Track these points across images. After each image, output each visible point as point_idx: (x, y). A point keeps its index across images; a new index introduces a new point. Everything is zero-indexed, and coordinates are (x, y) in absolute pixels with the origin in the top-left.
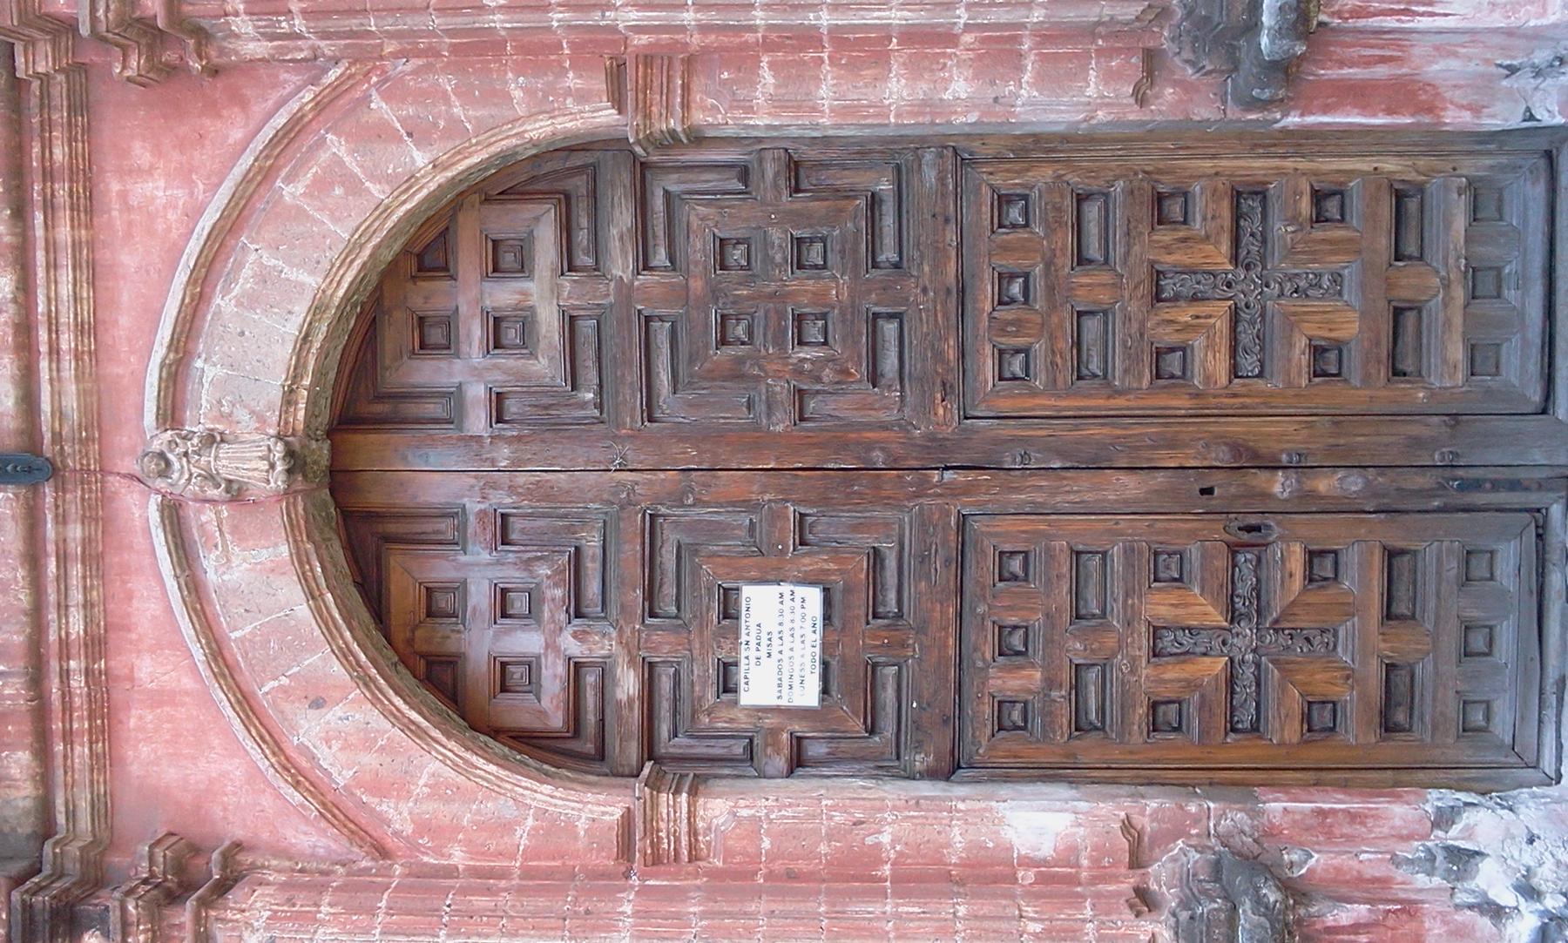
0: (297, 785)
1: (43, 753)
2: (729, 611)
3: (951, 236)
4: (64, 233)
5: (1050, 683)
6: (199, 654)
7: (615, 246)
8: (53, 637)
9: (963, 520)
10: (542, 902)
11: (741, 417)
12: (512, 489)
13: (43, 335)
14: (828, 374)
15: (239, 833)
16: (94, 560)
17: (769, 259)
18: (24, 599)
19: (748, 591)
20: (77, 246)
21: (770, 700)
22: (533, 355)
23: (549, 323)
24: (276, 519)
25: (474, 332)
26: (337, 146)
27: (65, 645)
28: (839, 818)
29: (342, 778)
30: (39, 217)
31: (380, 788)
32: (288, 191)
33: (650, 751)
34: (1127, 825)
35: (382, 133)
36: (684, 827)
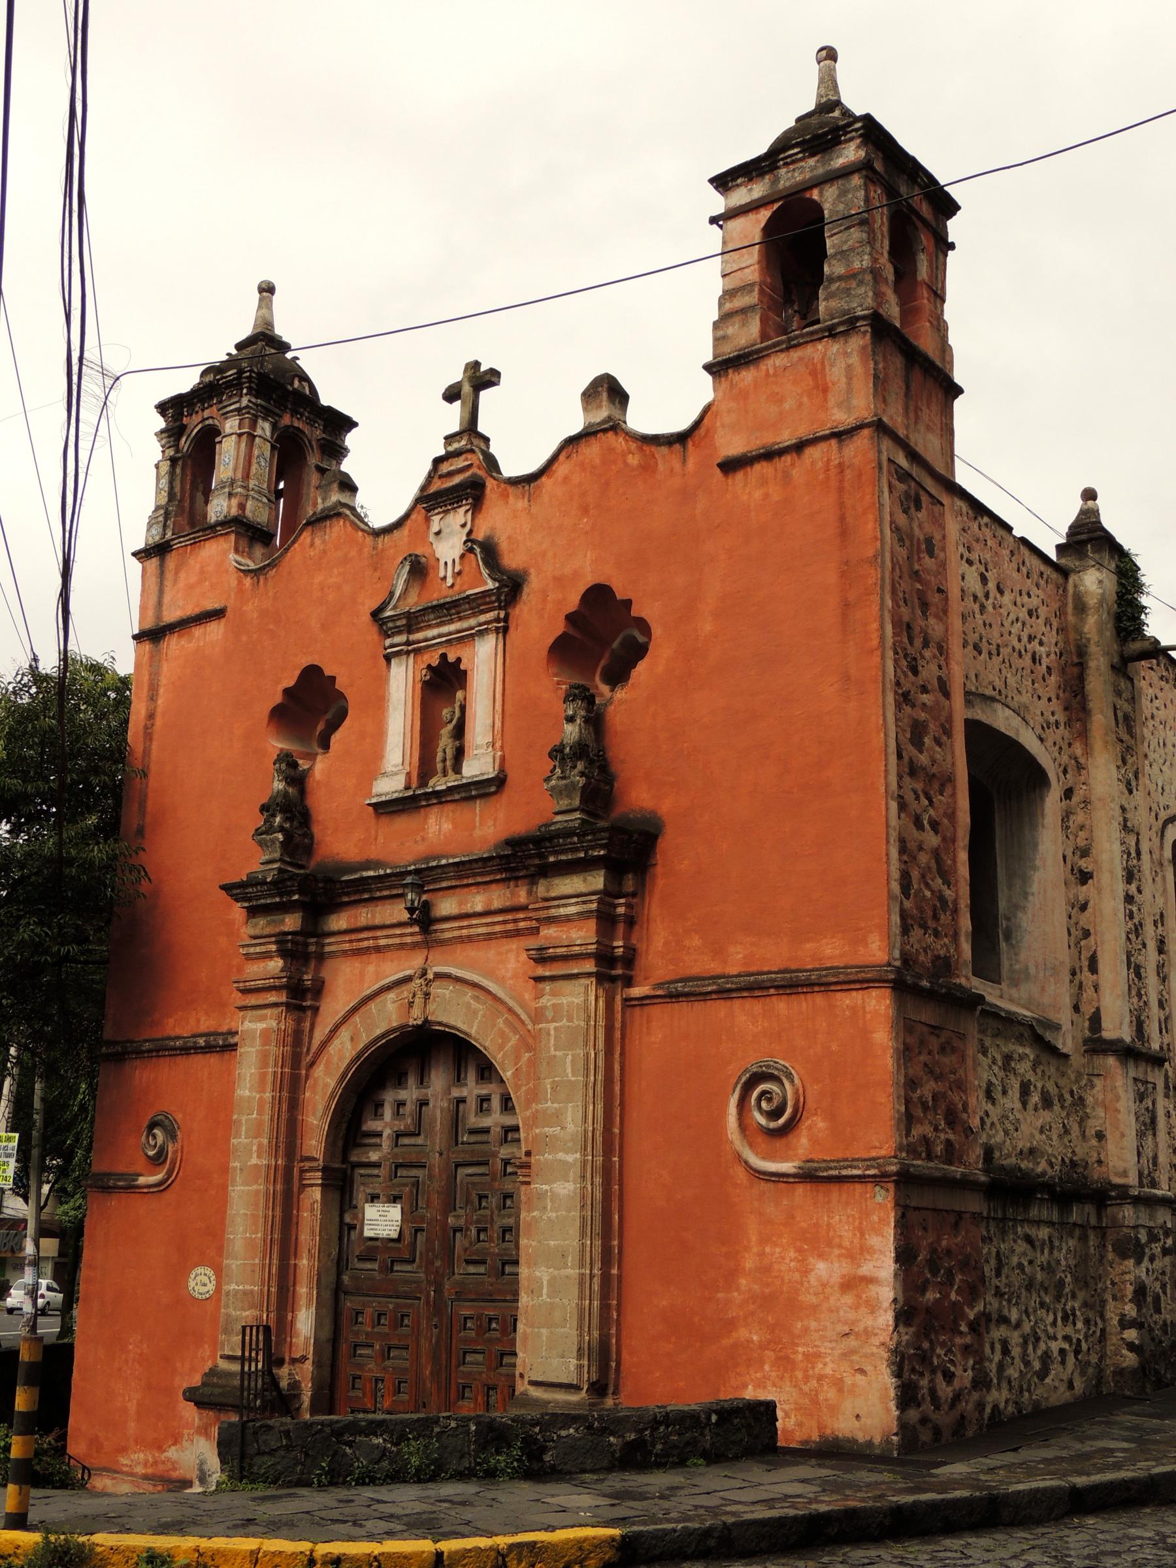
0: (331, 1031)
2: (395, 1199)
5: (367, 1334)
6: (368, 992)
7: (510, 1150)
8: (379, 933)
10: (283, 1129)
11: (458, 1206)
13: (465, 923)
15: (321, 1009)
16: (402, 946)
17: (504, 1217)
18: (388, 923)
19: (399, 1206)
20: (494, 933)
21: (367, 1216)
22: (476, 1114)
23: (486, 1122)
24: (403, 1021)
25: (484, 1092)
26: (514, 1040)
27: (376, 938)
30: (500, 918)
31: (328, 1063)
32: (500, 1021)
34: (303, 1359)
36: (312, 1182)
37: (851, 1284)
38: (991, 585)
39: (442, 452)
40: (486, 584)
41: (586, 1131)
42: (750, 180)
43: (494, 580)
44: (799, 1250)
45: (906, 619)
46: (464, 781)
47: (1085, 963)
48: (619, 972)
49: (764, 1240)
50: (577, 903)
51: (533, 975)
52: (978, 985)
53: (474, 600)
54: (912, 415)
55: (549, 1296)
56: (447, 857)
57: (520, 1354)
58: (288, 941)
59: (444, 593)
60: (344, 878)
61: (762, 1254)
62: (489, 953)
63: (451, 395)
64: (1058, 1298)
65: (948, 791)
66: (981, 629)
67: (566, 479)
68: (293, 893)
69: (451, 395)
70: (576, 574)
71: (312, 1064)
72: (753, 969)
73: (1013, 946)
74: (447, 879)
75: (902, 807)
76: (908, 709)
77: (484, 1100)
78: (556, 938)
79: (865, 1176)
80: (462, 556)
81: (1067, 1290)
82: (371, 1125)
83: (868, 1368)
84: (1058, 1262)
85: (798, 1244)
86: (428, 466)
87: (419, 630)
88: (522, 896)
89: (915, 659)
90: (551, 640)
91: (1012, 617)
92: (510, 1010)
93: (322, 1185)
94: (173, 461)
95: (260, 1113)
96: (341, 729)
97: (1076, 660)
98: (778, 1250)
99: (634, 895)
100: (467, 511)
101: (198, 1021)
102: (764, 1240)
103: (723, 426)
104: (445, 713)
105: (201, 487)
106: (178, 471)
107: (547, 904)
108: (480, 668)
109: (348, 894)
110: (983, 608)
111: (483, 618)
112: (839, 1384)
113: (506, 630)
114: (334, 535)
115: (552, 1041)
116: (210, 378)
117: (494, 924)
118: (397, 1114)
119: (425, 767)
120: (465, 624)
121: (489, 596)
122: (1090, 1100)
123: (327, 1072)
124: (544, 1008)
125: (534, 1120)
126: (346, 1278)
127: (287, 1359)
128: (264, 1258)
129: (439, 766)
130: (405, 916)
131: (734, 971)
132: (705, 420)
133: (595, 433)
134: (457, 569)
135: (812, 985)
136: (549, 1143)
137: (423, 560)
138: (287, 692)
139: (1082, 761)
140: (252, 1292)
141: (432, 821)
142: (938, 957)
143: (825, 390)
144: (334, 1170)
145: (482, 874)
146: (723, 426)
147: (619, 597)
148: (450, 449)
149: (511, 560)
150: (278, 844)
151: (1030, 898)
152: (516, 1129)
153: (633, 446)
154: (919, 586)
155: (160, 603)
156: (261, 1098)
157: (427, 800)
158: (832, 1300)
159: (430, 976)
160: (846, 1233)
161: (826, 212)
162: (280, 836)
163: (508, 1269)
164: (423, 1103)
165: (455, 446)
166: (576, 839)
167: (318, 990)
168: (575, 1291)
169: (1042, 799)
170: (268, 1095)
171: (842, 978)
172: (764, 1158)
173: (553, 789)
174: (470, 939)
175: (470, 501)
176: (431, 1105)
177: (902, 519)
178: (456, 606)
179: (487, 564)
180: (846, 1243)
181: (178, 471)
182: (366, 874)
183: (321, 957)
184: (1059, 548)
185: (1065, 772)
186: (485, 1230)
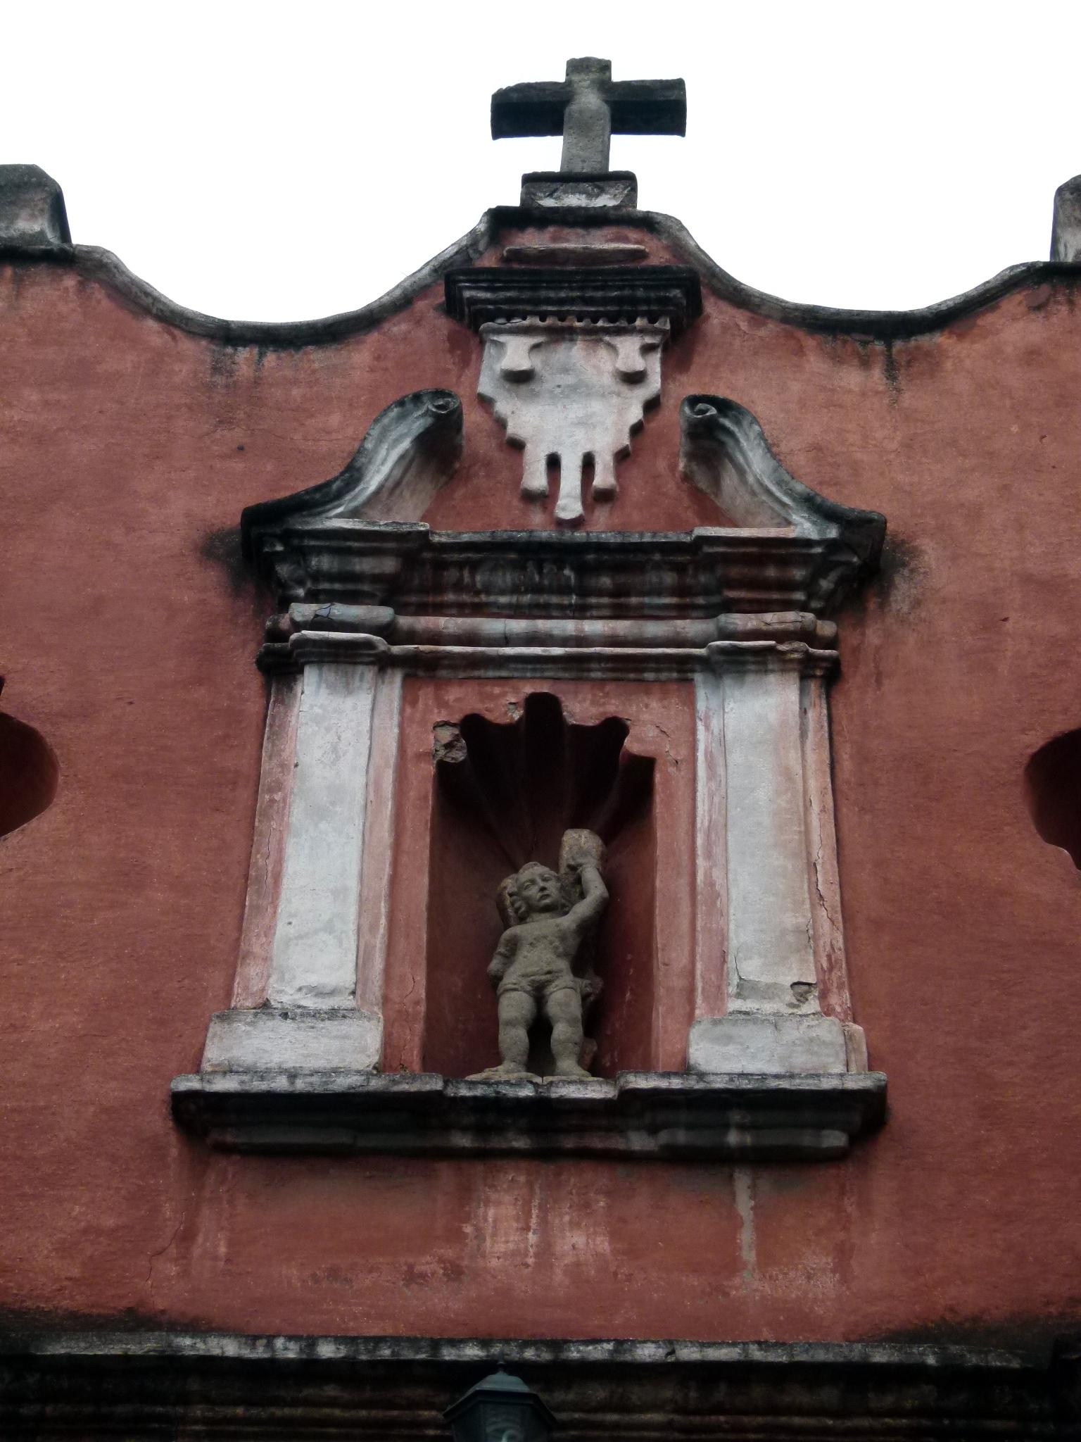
53: (726, 559)
60: (59, 1349)
80: (622, 457)
90: (1036, 740)
121: (784, 562)
134: (603, 478)
157: (481, 1130)
175: (665, 324)
178: (616, 569)
182: (187, 1344)
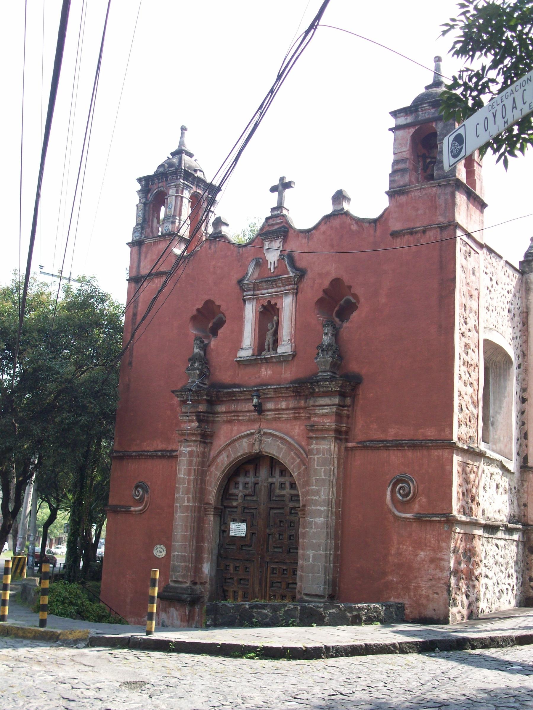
1: (225, 413)
2: (243, 521)
3: (292, 561)
4: (291, 415)
5: (231, 574)
6: (235, 438)
7: (294, 504)
8: (239, 414)
9: (253, 561)
11: (271, 525)
12: (261, 485)
13: (277, 413)
14: (274, 539)
15: (214, 443)
16: (249, 420)
18: (244, 410)
22: (279, 489)
23: (284, 492)
25: (282, 480)
26: (298, 460)
27: (238, 416)
28: (209, 537)
29: (218, 460)
31: (217, 466)
32: (292, 453)
33: (225, 507)
34: (206, 583)
35: (299, 468)
37: (432, 560)
38: (494, 282)
39: (269, 215)
40: (289, 274)
41: (329, 499)
42: (407, 115)
43: (293, 272)
44: (413, 547)
45: (464, 303)
46: (278, 355)
47: (523, 435)
48: (344, 437)
49: (399, 543)
50: (328, 409)
51: (308, 436)
52: (483, 447)
54: (469, 218)
55: (312, 561)
56: (271, 385)
57: (299, 584)
58: (200, 416)
59: (270, 275)
61: (398, 548)
62: (287, 426)
63: (273, 189)
64: (506, 569)
65: (477, 369)
66: (489, 301)
67: (324, 233)
68: (202, 396)
69: (273, 189)
70: (328, 274)
71: (209, 466)
72: (398, 438)
73: (494, 428)
74: (270, 394)
75: (460, 378)
76: (463, 338)
77: (282, 484)
78: (318, 422)
79: (441, 520)
80: (278, 260)
81: (510, 566)
82: (233, 491)
83: (439, 592)
84: (507, 555)
85: (413, 545)
86: (263, 221)
87: (259, 290)
88: (302, 403)
89: (466, 318)
90: (316, 299)
91: (502, 294)
92: (296, 449)
93: (214, 514)
94: (145, 204)
95: (189, 484)
96: (223, 328)
97: (525, 310)
98: (405, 547)
99: (349, 406)
100: (280, 242)
101: (158, 445)
102: (399, 543)
103: (392, 218)
104: (269, 325)
105: (156, 215)
106: (147, 209)
107: (314, 408)
108: (286, 308)
109: (226, 397)
110: (490, 291)
111: (287, 288)
112: (427, 598)
113: (297, 293)
114: (220, 245)
115: (316, 463)
116: (161, 170)
117: (289, 414)
118: (245, 488)
119: (260, 347)
120: (279, 290)
122: (522, 491)
123: (216, 469)
124: (312, 449)
125: (307, 493)
126: (222, 551)
127: (198, 582)
128: (190, 542)
129: (266, 347)
130: (253, 408)
131: (391, 439)
132: (385, 215)
133: (337, 215)
135: (422, 446)
136: (315, 503)
137: (261, 260)
138: (198, 310)
139: (526, 352)
140: (185, 556)
141: (263, 369)
142: (470, 437)
143: (436, 208)
144: (219, 509)
145: (285, 393)
146: (392, 218)
147: (346, 284)
148: (273, 214)
149: (301, 264)
150: (196, 375)
151: (503, 409)
152: (298, 496)
153: (354, 222)
154: (469, 288)
155: (139, 266)
156: (188, 479)
158: (426, 566)
159: (262, 433)
160: (433, 541)
161: (438, 133)
162: (198, 372)
163: (292, 551)
164: (256, 484)
165: (276, 213)
166: (328, 383)
167: (212, 436)
168: (324, 560)
169: (509, 369)
170: (192, 477)
171: (434, 444)
172: (400, 512)
173: (318, 362)
174: (279, 419)
175: (282, 237)
176: (260, 484)
177: (464, 262)
179: (290, 266)
180: (432, 545)
181: (147, 209)
182: (235, 390)
183: (213, 422)
184: (521, 263)
185: (518, 357)
186: (282, 535)
